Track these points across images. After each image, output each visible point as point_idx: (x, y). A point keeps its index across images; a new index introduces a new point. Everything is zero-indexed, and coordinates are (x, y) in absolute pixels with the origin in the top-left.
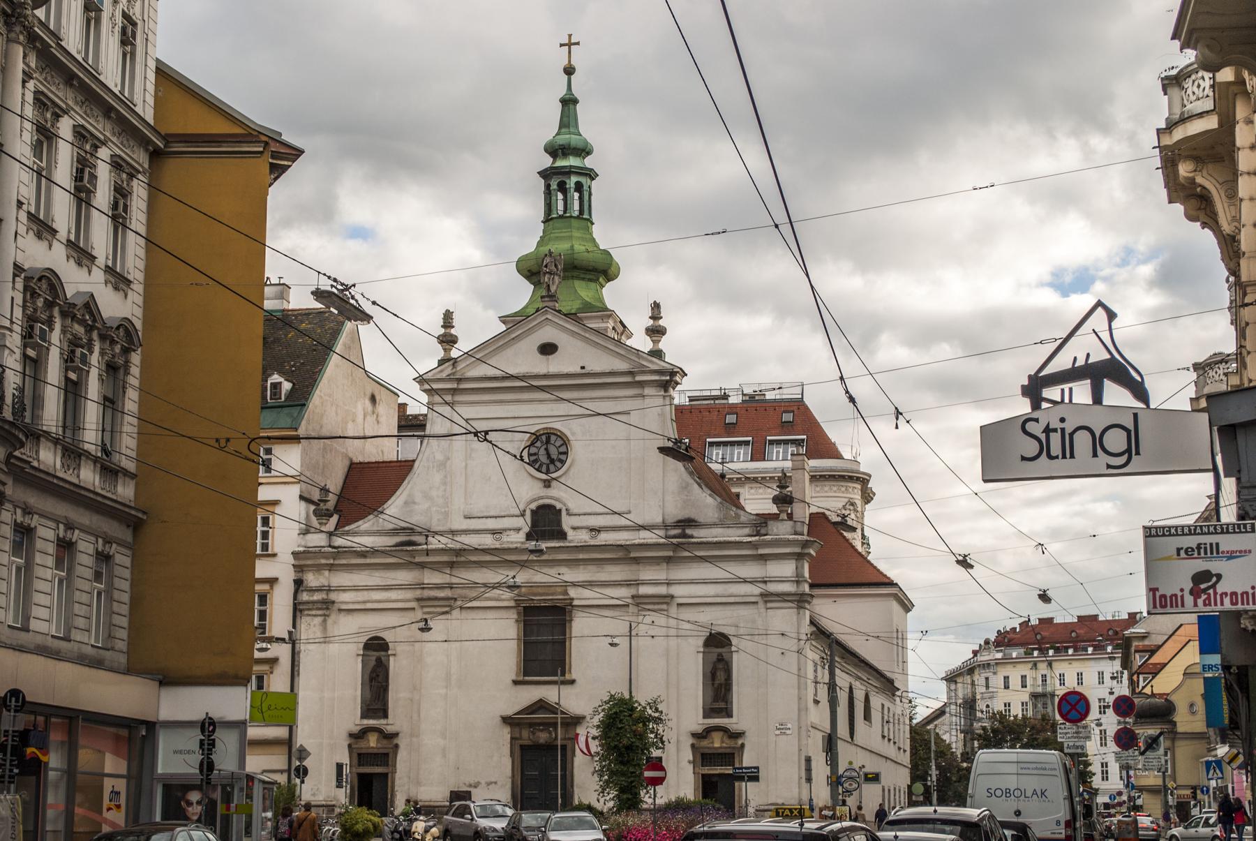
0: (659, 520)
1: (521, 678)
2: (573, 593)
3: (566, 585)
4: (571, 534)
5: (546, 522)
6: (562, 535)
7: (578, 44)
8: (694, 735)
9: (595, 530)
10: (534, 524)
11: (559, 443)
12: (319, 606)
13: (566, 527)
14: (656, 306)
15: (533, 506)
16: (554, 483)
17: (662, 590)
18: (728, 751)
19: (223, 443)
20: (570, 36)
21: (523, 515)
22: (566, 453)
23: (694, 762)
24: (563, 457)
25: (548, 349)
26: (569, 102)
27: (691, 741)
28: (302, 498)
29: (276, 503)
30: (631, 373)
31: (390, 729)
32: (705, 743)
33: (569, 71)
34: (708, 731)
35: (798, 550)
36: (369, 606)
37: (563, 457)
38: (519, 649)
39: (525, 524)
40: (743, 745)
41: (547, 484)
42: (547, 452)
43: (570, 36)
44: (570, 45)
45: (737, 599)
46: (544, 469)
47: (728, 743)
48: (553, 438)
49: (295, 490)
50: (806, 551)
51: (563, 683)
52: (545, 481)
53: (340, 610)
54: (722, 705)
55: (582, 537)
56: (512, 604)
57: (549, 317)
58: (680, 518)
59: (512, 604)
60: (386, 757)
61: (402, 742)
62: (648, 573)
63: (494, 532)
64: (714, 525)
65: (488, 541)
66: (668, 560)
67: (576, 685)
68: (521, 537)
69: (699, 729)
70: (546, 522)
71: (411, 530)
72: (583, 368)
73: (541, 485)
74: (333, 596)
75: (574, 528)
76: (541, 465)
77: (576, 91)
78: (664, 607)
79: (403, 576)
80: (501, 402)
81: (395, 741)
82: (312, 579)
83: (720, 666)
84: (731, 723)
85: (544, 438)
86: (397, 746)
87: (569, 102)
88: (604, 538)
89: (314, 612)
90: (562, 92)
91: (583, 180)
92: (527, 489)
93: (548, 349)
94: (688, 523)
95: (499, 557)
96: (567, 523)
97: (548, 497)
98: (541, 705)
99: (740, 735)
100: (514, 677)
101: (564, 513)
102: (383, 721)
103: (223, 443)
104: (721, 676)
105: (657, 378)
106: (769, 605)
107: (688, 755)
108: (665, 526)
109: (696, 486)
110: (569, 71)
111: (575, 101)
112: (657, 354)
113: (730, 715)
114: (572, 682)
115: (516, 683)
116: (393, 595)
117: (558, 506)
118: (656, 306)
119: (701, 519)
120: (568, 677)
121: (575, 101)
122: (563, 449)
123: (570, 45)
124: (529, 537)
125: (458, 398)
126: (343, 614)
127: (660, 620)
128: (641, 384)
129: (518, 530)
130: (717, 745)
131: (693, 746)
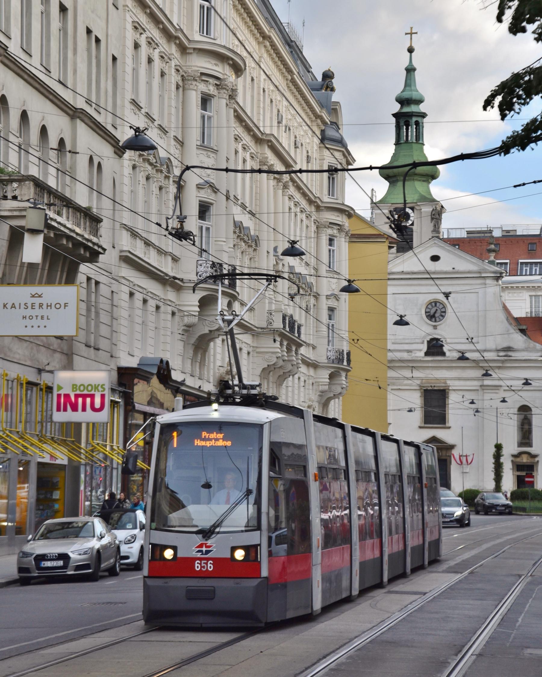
0: (494, 347)
1: (423, 425)
2: (449, 382)
3: (445, 379)
4: (448, 354)
5: (435, 348)
6: (443, 354)
8: (513, 456)
10: (429, 348)
11: (441, 306)
13: (445, 349)
16: (438, 327)
18: (530, 464)
19: (356, 341)
20: (411, 28)
21: (423, 343)
22: (445, 312)
23: (513, 469)
24: (443, 314)
25: (435, 258)
26: (410, 70)
30: (480, 273)
32: (518, 460)
33: (411, 50)
34: (520, 454)
37: (443, 314)
39: (425, 347)
40: (538, 462)
41: (435, 327)
42: (435, 313)
43: (411, 28)
44: (411, 34)
54: (527, 441)
56: (418, 388)
57: (436, 242)
63: (409, 351)
64: (523, 350)
65: (405, 356)
68: (422, 354)
70: (435, 348)
72: (453, 269)
73: (432, 328)
75: (449, 350)
77: (415, 64)
80: (411, 285)
83: (526, 421)
85: (433, 304)
87: (410, 70)
90: (406, 64)
91: (419, 119)
93: (435, 258)
94: (509, 349)
95: (412, 365)
97: (436, 334)
99: (535, 456)
103: (356, 341)
110: (411, 50)
111: (414, 70)
114: (449, 428)
115: (420, 427)
119: (515, 347)
120: (447, 425)
121: (414, 70)
122: (443, 310)
123: (411, 34)
124: (427, 354)
129: (421, 350)
131: (512, 461)
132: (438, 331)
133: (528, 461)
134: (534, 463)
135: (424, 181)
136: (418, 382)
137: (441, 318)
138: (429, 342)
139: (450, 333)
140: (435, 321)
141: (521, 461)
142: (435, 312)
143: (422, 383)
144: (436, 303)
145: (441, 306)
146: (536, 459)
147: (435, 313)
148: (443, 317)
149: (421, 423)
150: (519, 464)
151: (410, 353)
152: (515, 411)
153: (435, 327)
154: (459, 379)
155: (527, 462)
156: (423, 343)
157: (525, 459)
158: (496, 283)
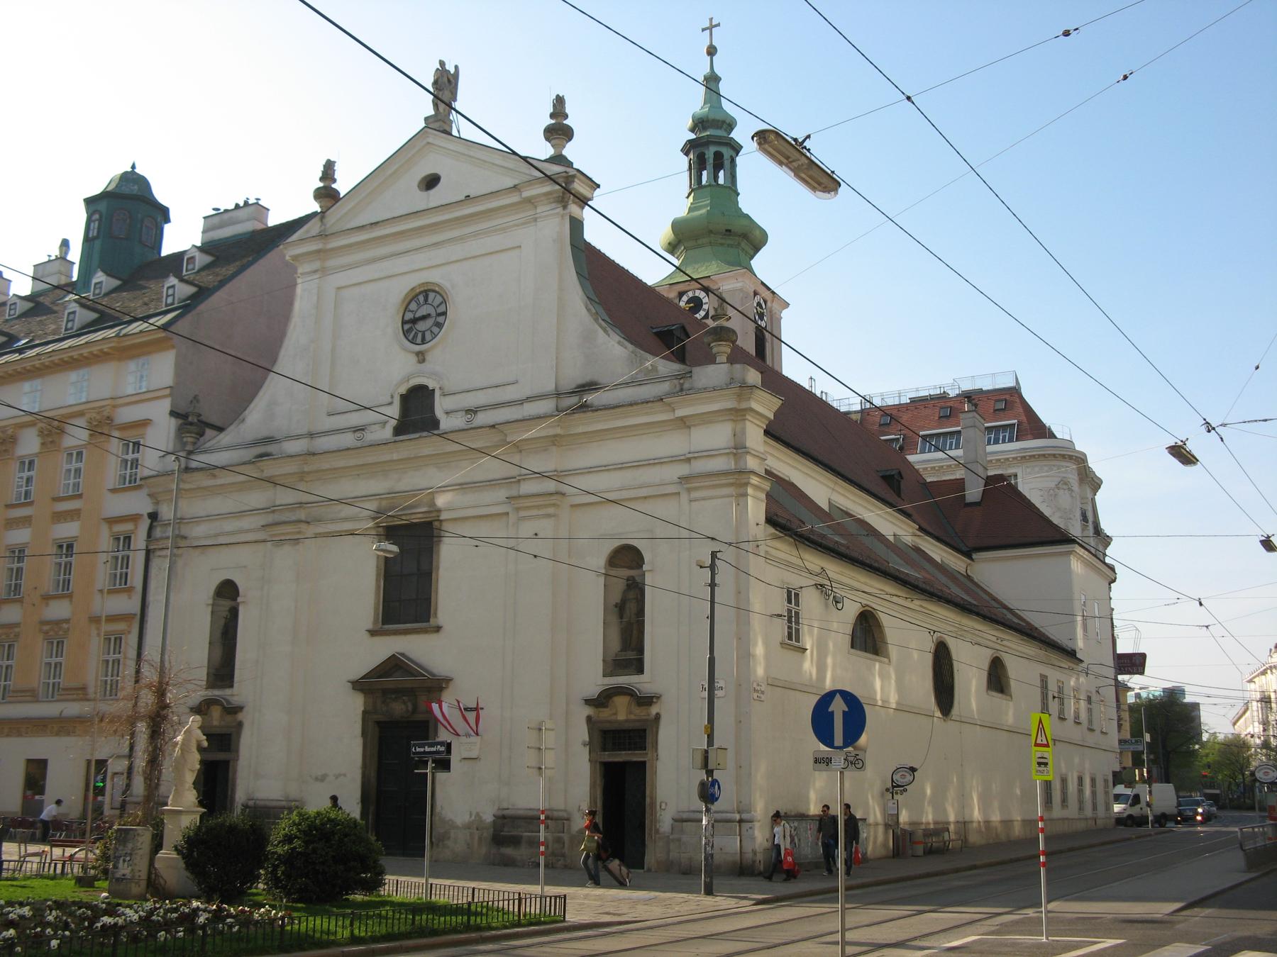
0: (550, 387)
2: (441, 501)
4: (446, 423)
5: (416, 411)
6: (435, 424)
7: (718, 25)
8: (588, 702)
9: (472, 411)
11: (439, 299)
13: (439, 413)
14: (559, 101)
15: (403, 390)
16: (428, 357)
17: (551, 486)
20: (711, 19)
22: (444, 314)
23: (590, 744)
24: (441, 319)
25: (431, 182)
26: (712, 81)
28: (173, 413)
29: (145, 423)
31: (236, 700)
32: (605, 714)
33: (712, 51)
35: (730, 404)
36: (222, 540)
38: (378, 587)
40: (658, 717)
41: (421, 357)
42: (422, 317)
43: (711, 19)
44: (711, 28)
46: (419, 340)
47: (639, 713)
48: (431, 295)
49: (166, 405)
50: (744, 405)
51: (425, 631)
52: (418, 354)
54: (631, 655)
55: (457, 421)
57: (430, 140)
58: (580, 381)
62: (537, 463)
64: (627, 384)
65: (348, 440)
66: (555, 440)
67: (442, 634)
68: (387, 433)
69: (593, 690)
70: (416, 411)
71: (270, 440)
73: (414, 359)
74: (185, 530)
76: (415, 336)
78: (551, 510)
79: (257, 498)
81: (240, 716)
82: (166, 512)
84: (643, 683)
85: (421, 298)
86: (240, 725)
88: (482, 418)
92: (395, 368)
93: (431, 182)
94: (590, 387)
96: (441, 406)
98: (395, 665)
100: (370, 626)
101: (437, 394)
102: (228, 692)
104: (631, 607)
106: (695, 495)
107: (583, 733)
108: (558, 395)
109: (601, 332)
110: (712, 51)
112: (559, 159)
113: (640, 670)
114: (438, 629)
115: (373, 633)
116: (246, 523)
117: (431, 384)
118: (559, 101)
123: (711, 28)
124: (398, 431)
125: (331, 263)
127: (545, 527)
128: (530, 201)
130: (622, 717)
131: (589, 719)
132: (427, 366)
133: (632, 717)
134: (646, 720)
135: (730, 246)
137: (435, 330)
138: (405, 399)
139: (456, 369)
140: (424, 341)
141: (613, 718)
142: (424, 318)
144: (426, 293)
146: (654, 710)
147: (422, 317)
148: (440, 326)
149: (375, 622)
150: (607, 727)
151: (358, 434)
152: (598, 561)
153: (421, 357)
155: (626, 721)
156: (390, 404)
157: (621, 712)
158: (560, 210)
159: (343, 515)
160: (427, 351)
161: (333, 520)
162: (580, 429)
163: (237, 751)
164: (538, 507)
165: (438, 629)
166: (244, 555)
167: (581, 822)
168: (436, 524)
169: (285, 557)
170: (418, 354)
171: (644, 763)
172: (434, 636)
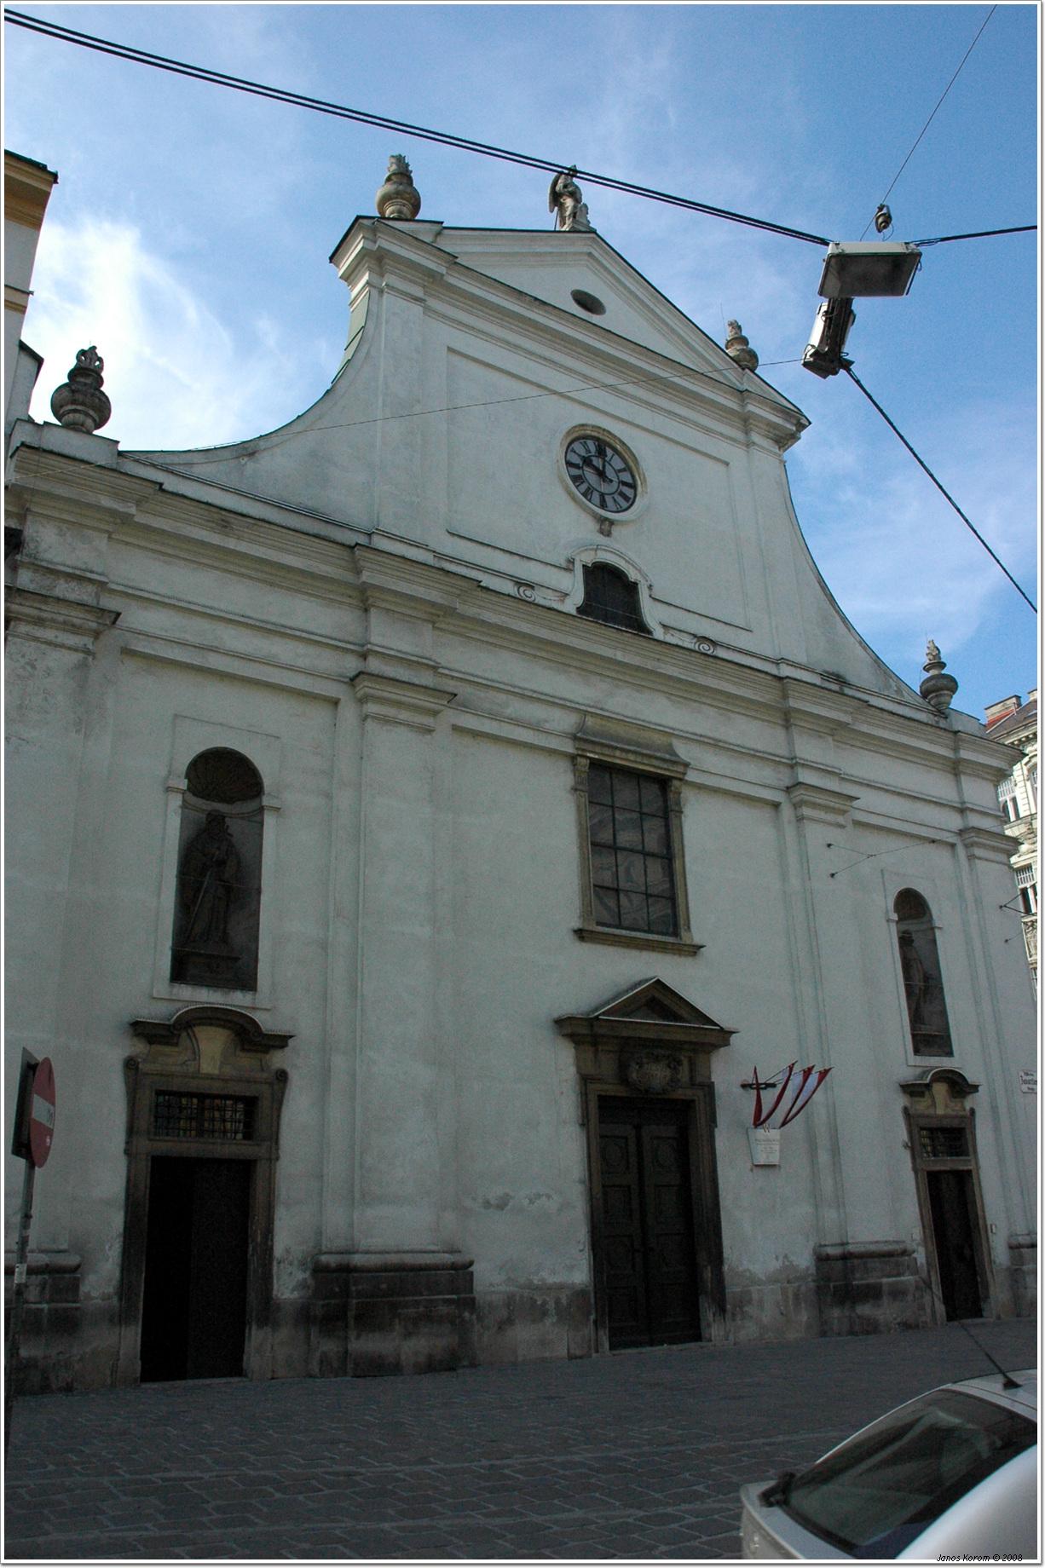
2: (683, 751)
3: (670, 734)
12: (77, 617)
16: (615, 530)
23: (912, 1148)
27: (901, 1100)
37: (629, 492)
40: (973, 1111)
41: (606, 527)
45: (924, 832)
52: (602, 520)
53: (127, 652)
59: (569, 748)
60: (254, 1110)
61: (298, 1063)
63: (519, 583)
69: (908, 1074)
73: (592, 525)
81: (277, 1059)
86: (282, 1077)
89: (49, 634)
105: (780, 421)
113: (950, 1054)
114: (694, 950)
115: (581, 934)
117: (633, 575)
126: (131, 664)
133: (949, 1111)
134: (963, 1117)
136: (566, 722)
141: (931, 1111)
143: (582, 727)
145: (618, 463)
153: (606, 527)
154: (716, 745)
155: (945, 1116)
157: (941, 1104)
159: (509, 711)
160: (622, 523)
161: (494, 717)
162: (865, 728)
163: (275, 1138)
164: (827, 809)
165: (694, 950)
166: (271, 713)
167: (921, 1256)
168: (676, 783)
169: (396, 751)
170: (602, 520)
171: (969, 1172)
172: (686, 962)
